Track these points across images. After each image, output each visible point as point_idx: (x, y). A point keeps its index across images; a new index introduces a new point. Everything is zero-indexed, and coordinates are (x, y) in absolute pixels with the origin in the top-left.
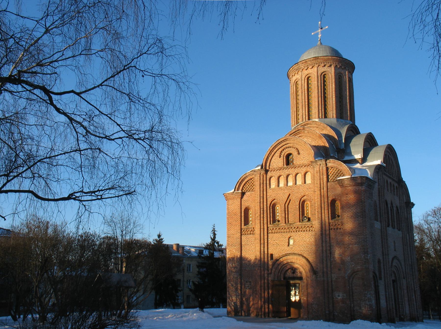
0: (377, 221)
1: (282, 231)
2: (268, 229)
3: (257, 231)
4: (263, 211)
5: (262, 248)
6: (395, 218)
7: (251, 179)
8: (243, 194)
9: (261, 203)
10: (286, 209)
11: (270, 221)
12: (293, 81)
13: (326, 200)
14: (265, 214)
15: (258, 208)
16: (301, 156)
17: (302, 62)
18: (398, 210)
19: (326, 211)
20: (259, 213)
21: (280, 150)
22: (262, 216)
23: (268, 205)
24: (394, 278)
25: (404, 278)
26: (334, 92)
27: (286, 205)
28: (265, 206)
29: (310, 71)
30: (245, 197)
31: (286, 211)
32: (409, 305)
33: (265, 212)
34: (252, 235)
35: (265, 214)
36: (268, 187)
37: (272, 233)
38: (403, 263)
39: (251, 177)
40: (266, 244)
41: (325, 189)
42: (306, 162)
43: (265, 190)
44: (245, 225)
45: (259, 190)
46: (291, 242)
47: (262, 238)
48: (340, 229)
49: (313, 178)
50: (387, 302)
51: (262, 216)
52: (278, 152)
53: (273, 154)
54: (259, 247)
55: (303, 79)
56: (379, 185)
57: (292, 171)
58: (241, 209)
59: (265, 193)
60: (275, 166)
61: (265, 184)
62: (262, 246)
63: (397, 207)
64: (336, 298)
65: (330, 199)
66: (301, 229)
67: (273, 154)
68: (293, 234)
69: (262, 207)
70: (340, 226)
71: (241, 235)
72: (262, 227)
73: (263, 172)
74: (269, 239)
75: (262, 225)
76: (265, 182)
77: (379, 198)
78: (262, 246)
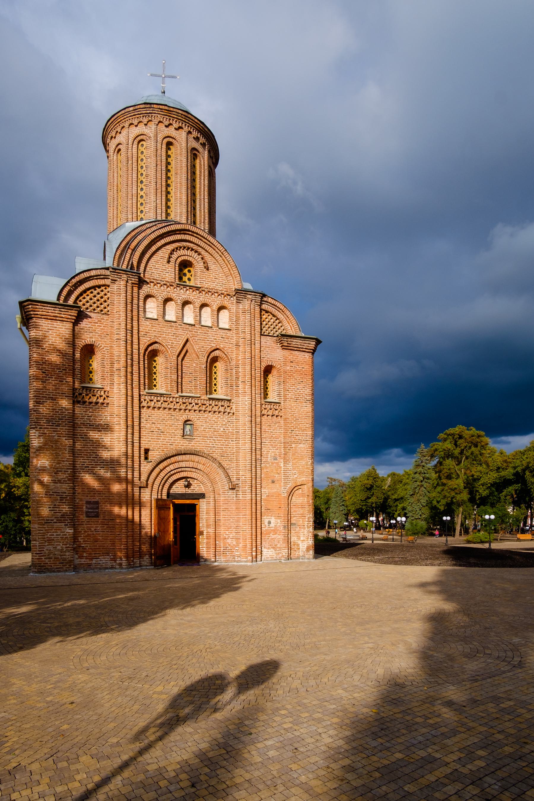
4: (132, 360)
5: (130, 436)
14: (135, 368)
16: (212, 274)
17: (161, 107)
22: (129, 370)
23: (142, 351)
28: (135, 351)
33: (135, 363)
35: (135, 368)
40: (136, 428)
47: (130, 415)
51: (129, 370)
54: (123, 433)
62: (130, 431)
69: (129, 352)
74: (142, 420)
75: (129, 387)
78: (130, 431)
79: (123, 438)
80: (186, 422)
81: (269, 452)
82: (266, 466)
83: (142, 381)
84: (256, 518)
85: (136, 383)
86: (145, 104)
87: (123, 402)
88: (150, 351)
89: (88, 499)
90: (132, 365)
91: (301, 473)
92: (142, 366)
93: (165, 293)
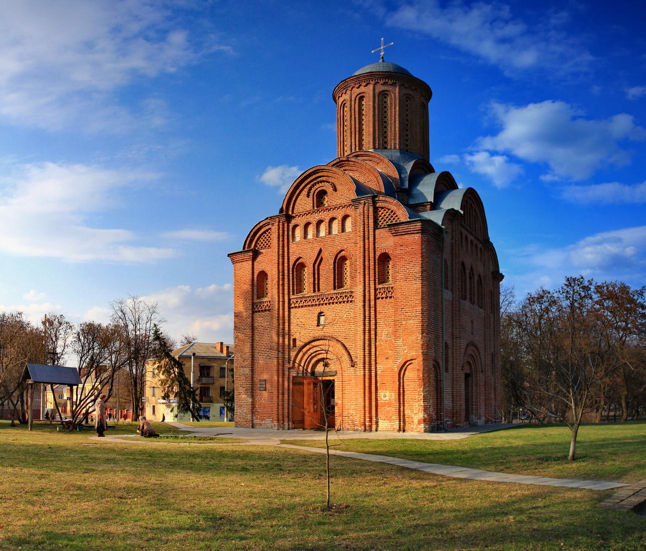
0: (447, 289)
1: (310, 304)
2: (289, 303)
4: (283, 275)
6: (476, 288)
7: (267, 230)
9: (281, 263)
10: (316, 271)
11: (293, 290)
12: (340, 104)
13: (372, 255)
14: (286, 280)
16: (339, 193)
18: (481, 279)
19: (372, 272)
20: (277, 279)
21: (309, 186)
22: (281, 283)
23: (291, 267)
24: (468, 372)
25: (482, 372)
28: (286, 268)
30: (259, 258)
32: (485, 405)
33: (286, 277)
34: (268, 312)
35: (286, 280)
36: (291, 240)
37: (296, 307)
38: (482, 352)
41: (371, 239)
42: (345, 202)
43: (286, 245)
44: (258, 298)
45: (277, 245)
46: (322, 318)
48: (390, 297)
49: (354, 224)
50: (453, 402)
52: (306, 190)
53: (298, 192)
56: (452, 239)
57: (326, 216)
58: (253, 274)
59: (286, 249)
60: (301, 210)
61: (286, 237)
63: (479, 276)
64: (381, 398)
65: (378, 254)
66: (336, 301)
67: (298, 192)
68: (323, 308)
69: (281, 270)
70: (390, 293)
71: (253, 312)
72: (281, 299)
73: (283, 219)
76: (286, 233)
77: (452, 257)
81: (384, 332)
82: (380, 344)
85: (286, 291)
86: (342, 82)
88: (298, 265)
90: (283, 279)
91: (411, 348)
93: (305, 220)
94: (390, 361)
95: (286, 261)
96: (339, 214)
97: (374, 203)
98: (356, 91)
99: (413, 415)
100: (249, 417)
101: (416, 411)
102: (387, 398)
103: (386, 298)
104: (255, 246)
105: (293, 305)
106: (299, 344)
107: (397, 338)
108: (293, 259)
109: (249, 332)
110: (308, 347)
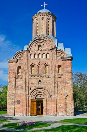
1: (36, 77)
3: (24, 77)
5: (26, 85)
7: (22, 54)
8: (17, 61)
10: (38, 68)
15: (24, 67)
16: (45, 46)
21: (36, 43)
22: (26, 70)
23: (30, 66)
26: (52, 26)
27: (38, 66)
29: (43, 16)
31: (38, 69)
34: (21, 79)
36: (30, 58)
39: (22, 53)
40: (28, 83)
42: (47, 49)
49: (51, 56)
55: (40, 19)
57: (42, 52)
65: (58, 65)
68: (40, 79)
79: (25, 86)
80: (40, 81)
81: (60, 87)
83: (29, 72)
84: (56, 104)
87: (25, 78)
89: (18, 99)
92: (29, 69)
94: (62, 95)
95: (28, 64)
96: (46, 52)
97: (57, 50)
98: (42, 17)
99: (69, 111)
100: (13, 112)
101: (71, 110)
102: (61, 106)
103: (61, 77)
104: (17, 58)
105: (30, 77)
106: (32, 89)
107: (64, 89)
108: (30, 64)
109: (14, 84)
110: (35, 91)
